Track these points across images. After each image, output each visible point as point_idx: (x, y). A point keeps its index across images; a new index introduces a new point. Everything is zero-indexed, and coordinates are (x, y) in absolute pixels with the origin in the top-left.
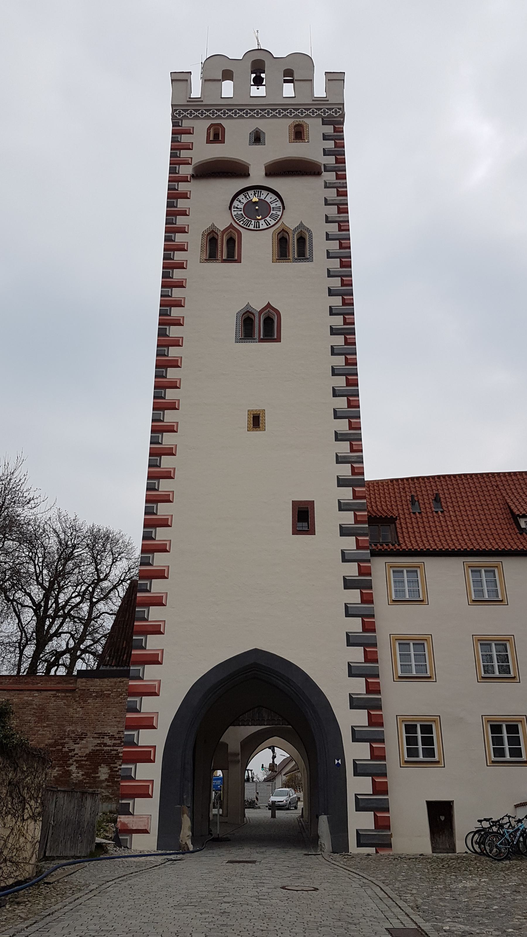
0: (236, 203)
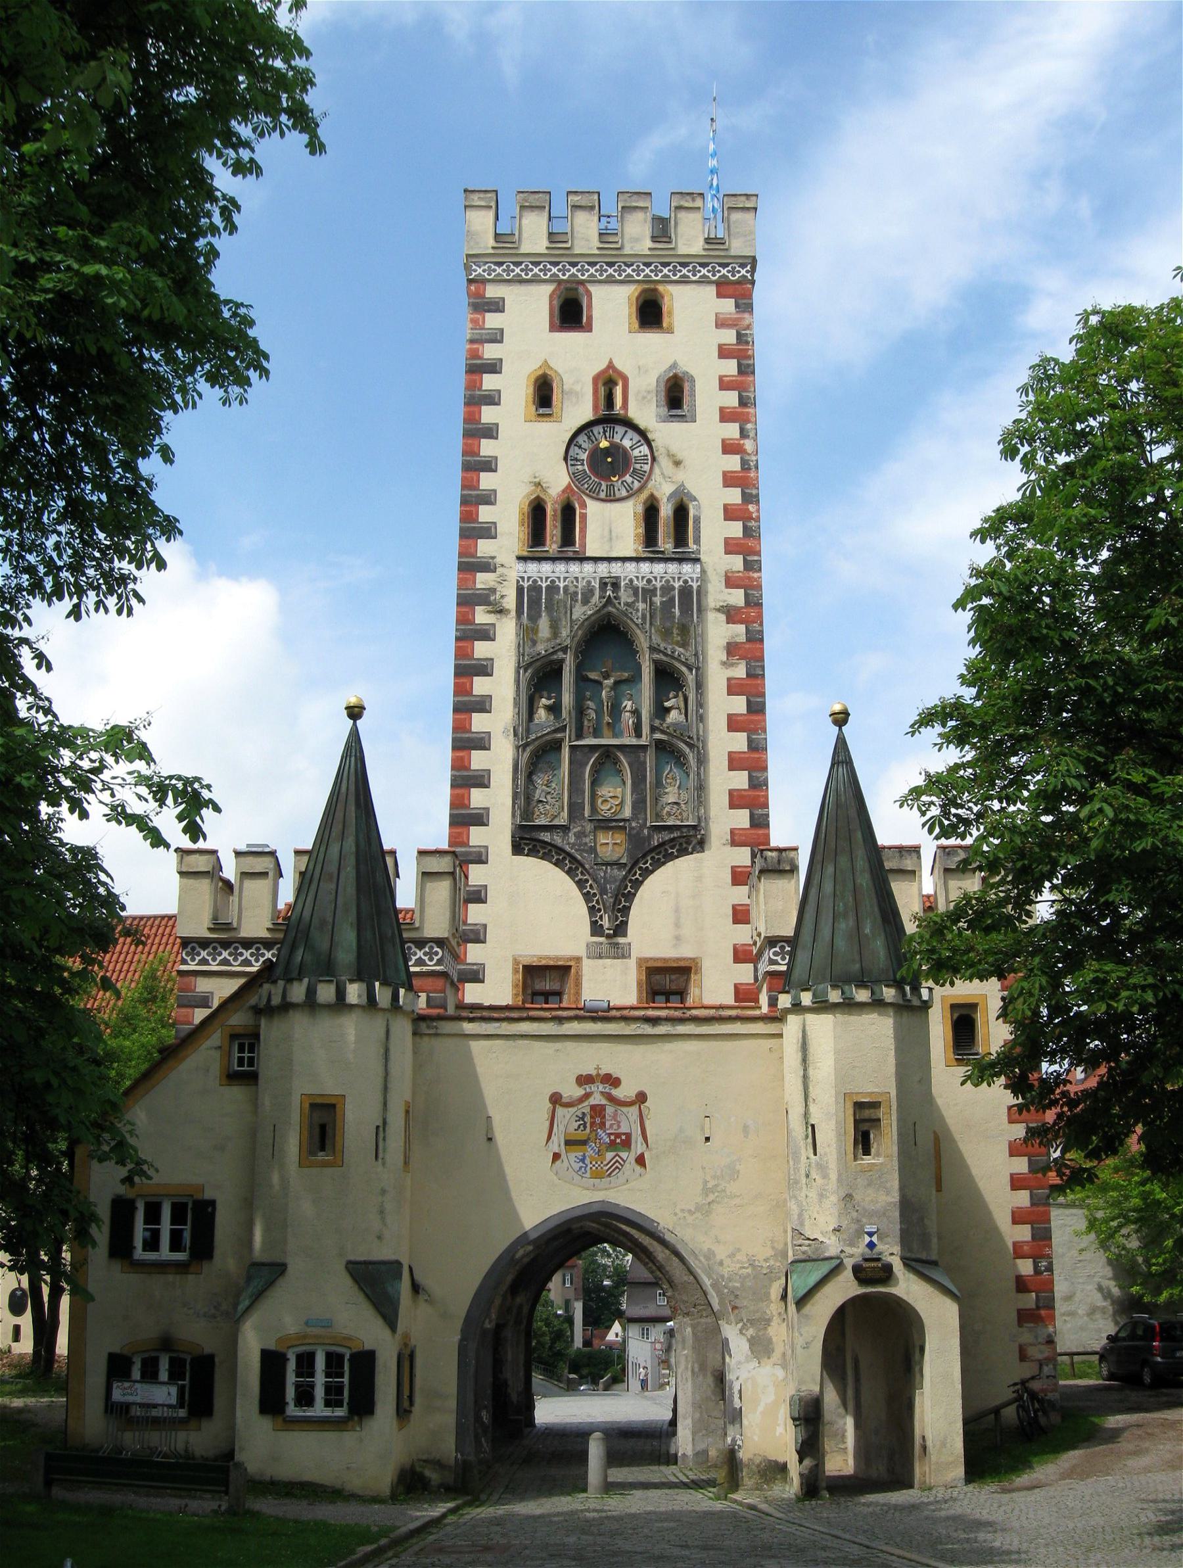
0: (574, 451)
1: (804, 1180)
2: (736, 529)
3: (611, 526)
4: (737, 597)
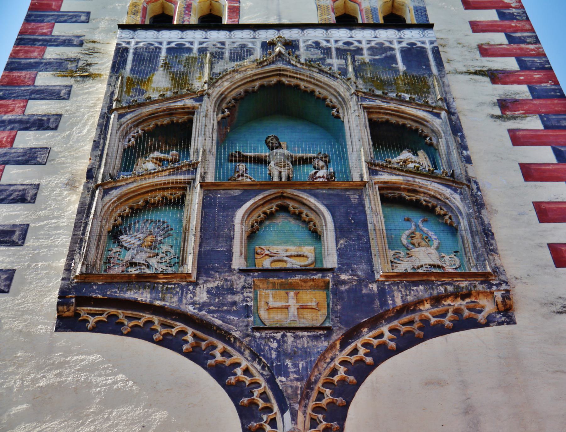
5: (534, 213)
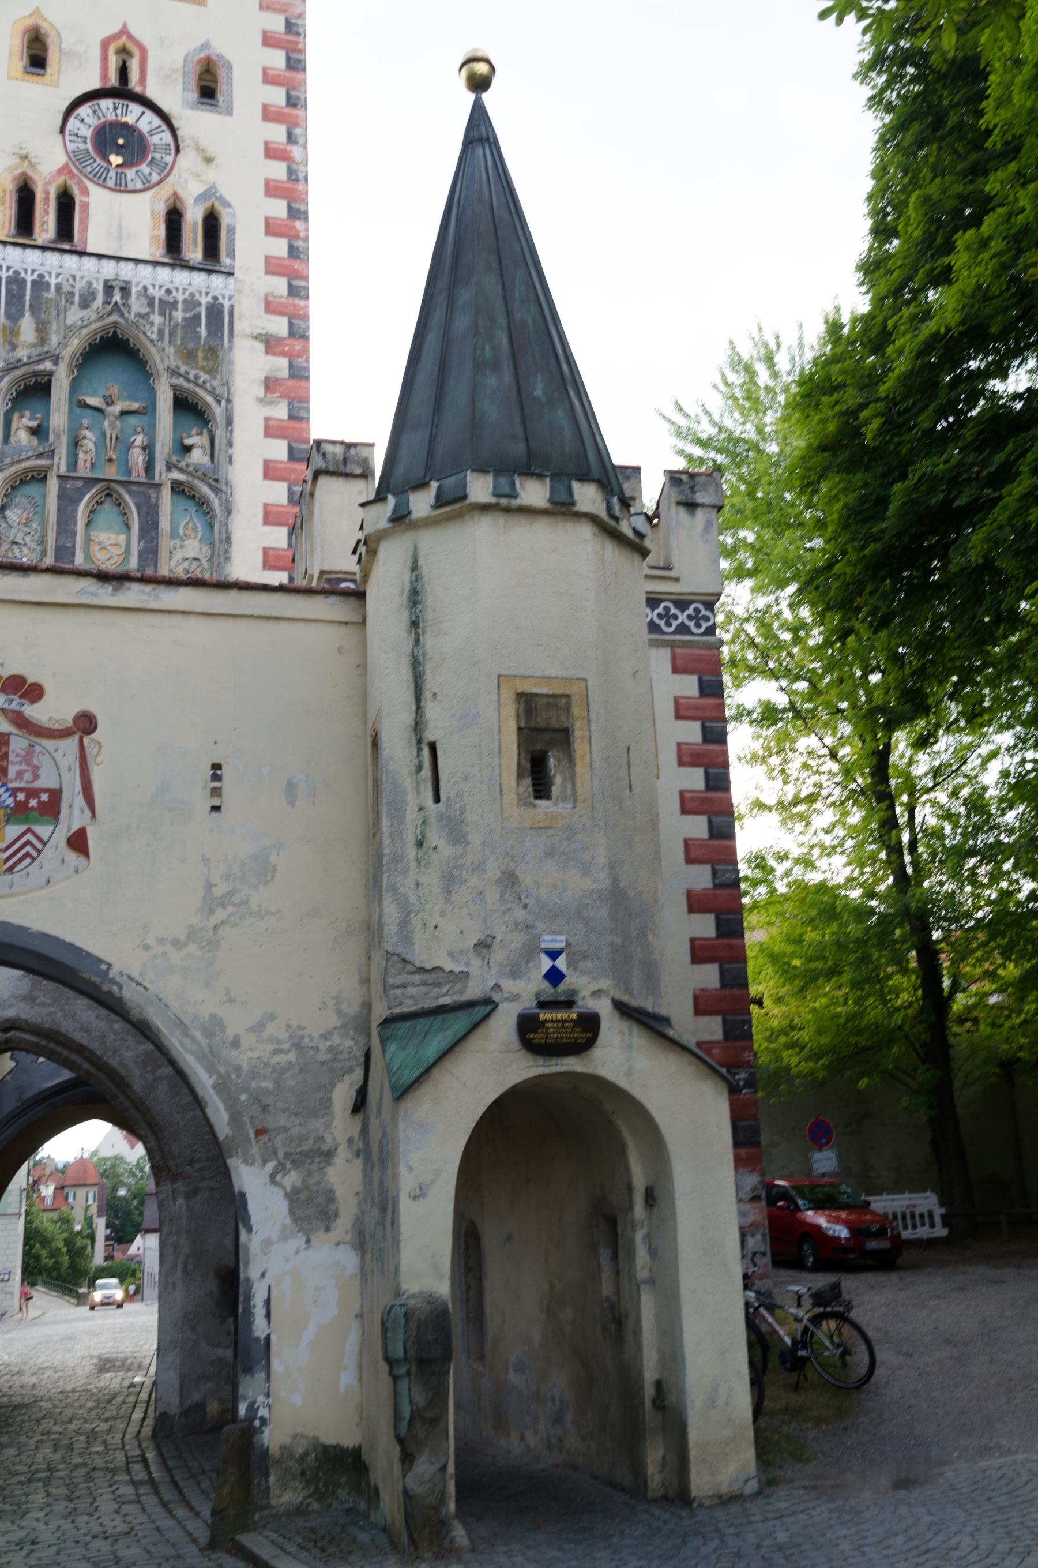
0: (72, 124)
1: (411, 853)
2: (279, 247)
3: (121, 221)
4: (279, 326)
5: (261, 516)
